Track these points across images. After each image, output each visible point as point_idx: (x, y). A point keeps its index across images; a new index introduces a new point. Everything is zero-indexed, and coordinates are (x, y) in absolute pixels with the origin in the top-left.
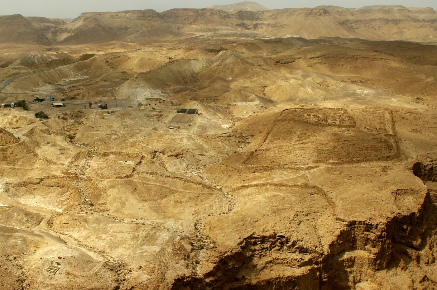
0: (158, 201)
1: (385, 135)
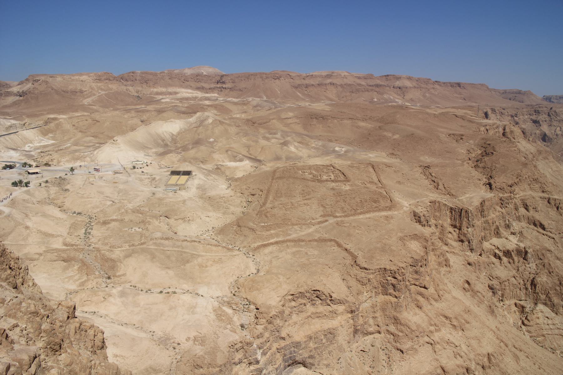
1: (377, 188)
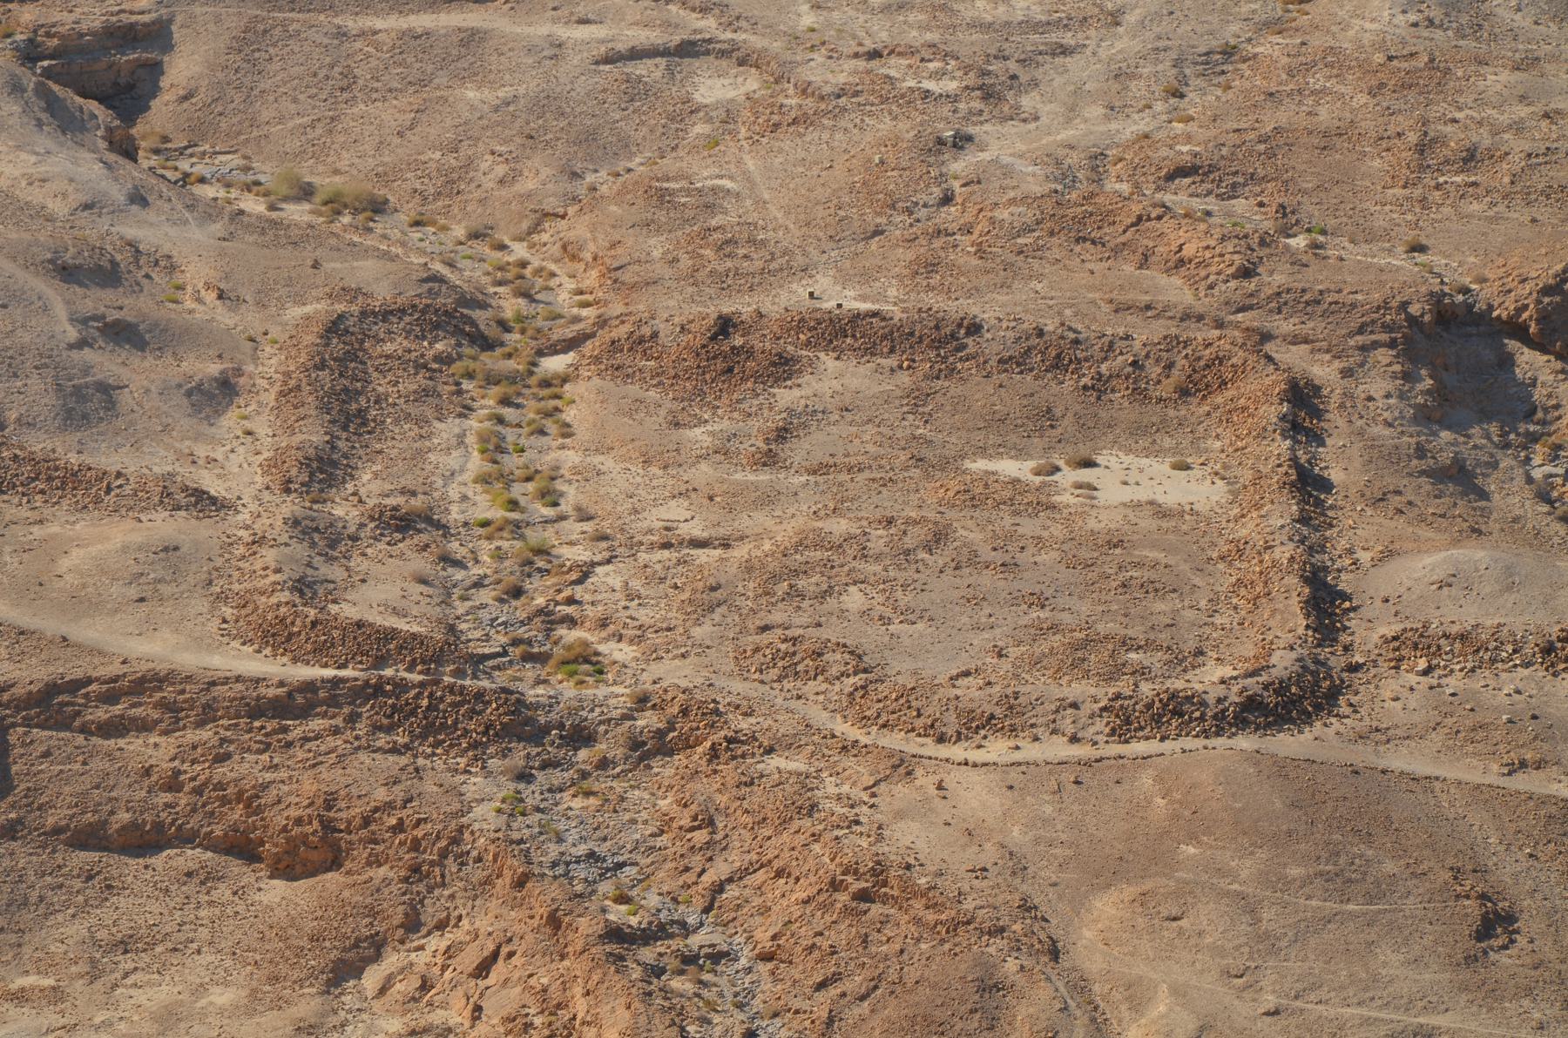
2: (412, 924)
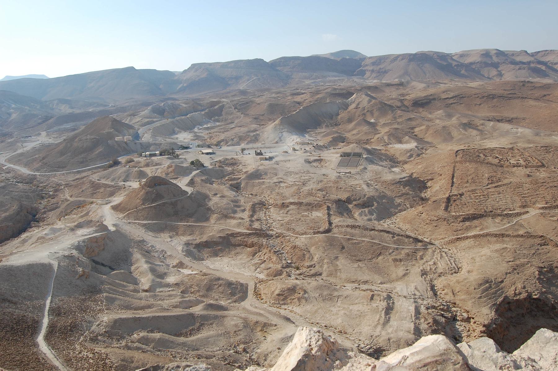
0: (374, 260)
2: (259, 251)
